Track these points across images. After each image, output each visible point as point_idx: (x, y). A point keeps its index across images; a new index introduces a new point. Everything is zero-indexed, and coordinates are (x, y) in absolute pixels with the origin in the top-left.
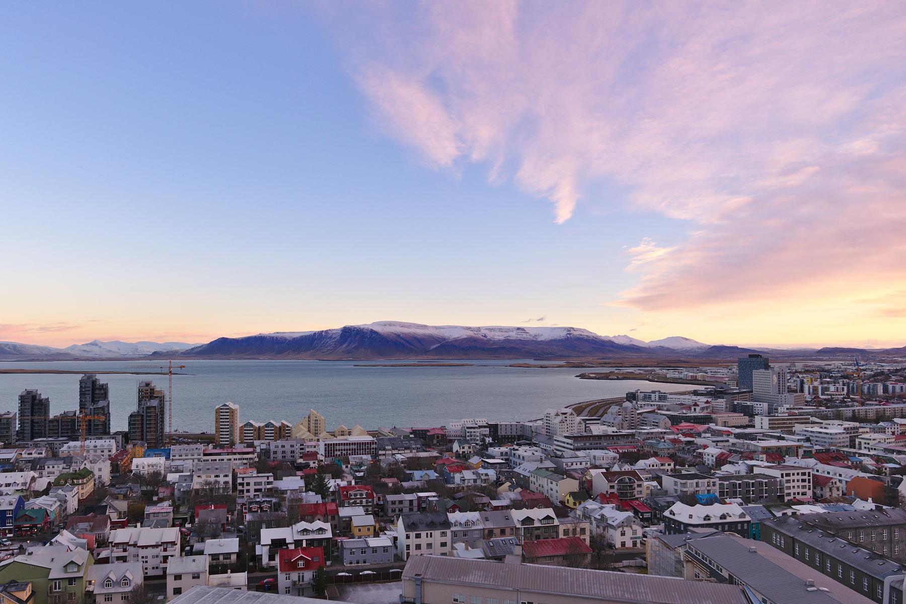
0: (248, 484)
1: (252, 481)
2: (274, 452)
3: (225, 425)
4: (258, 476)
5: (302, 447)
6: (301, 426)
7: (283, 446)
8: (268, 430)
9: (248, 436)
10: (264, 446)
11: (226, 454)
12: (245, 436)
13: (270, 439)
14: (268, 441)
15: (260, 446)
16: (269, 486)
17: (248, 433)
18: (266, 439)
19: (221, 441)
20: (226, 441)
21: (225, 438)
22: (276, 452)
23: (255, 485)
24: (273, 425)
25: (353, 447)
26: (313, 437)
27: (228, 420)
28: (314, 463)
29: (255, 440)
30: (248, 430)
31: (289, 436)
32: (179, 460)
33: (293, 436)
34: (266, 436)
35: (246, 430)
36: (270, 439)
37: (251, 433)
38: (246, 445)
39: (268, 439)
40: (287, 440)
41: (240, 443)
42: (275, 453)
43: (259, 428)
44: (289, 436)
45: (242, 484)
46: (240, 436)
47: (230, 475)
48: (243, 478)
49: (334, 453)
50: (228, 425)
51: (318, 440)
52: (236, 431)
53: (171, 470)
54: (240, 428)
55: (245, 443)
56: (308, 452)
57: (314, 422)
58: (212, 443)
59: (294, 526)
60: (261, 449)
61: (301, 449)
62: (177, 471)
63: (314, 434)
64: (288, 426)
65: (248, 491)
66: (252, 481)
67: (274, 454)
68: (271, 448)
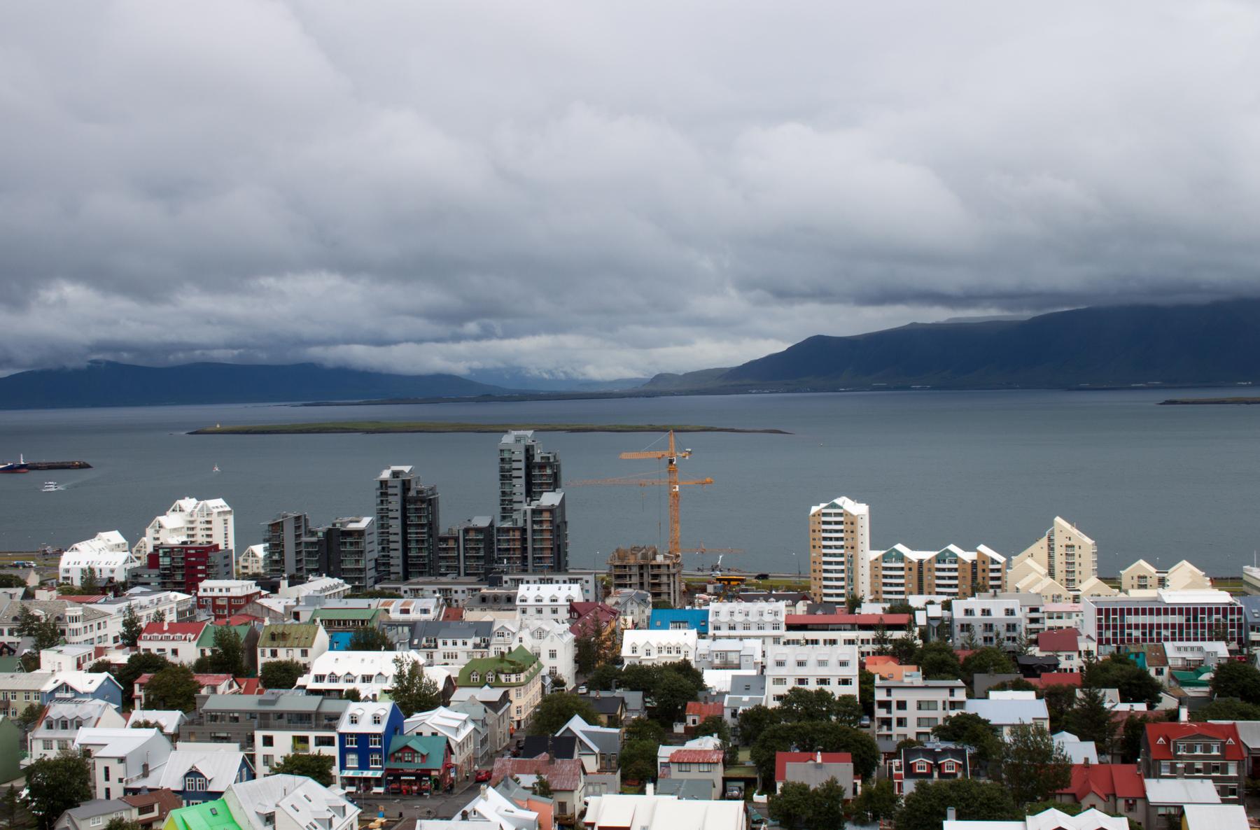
0: (902, 705)
1: (911, 698)
2: (962, 626)
3: (834, 555)
4: (926, 687)
5: (1034, 615)
6: (1029, 561)
7: (986, 612)
8: (944, 570)
9: (891, 585)
10: (936, 611)
11: (849, 627)
12: (885, 584)
13: (949, 594)
14: (945, 598)
15: (925, 609)
16: (953, 713)
17: (891, 577)
18: (938, 593)
19: (826, 595)
20: (838, 595)
21: (837, 587)
22: (968, 625)
23: (919, 708)
24: (955, 555)
25: (1171, 619)
26: (1061, 590)
27: (841, 543)
28: (1068, 658)
29: (911, 593)
30: (891, 569)
31: (999, 587)
32: (729, 637)
33: (1009, 586)
34: (938, 586)
35: (885, 569)
36: (949, 594)
37: (902, 577)
38: (887, 606)
39: (942, 593)
40: (995, 595)
41: (872, 601)
42: (966, 627)
43: (921, 562)
44: (999, 587)
45: (886, 705)
46: (872, 584)
47: (856, 681)
48: (889, 690)
49: (1115, 634)
50: (842, 555)
51: (1076, 599)
52: (861, 571)
53: (711, 662)
54: (871, 562)
55: (885, 601)
56: (1051, 629)
57: (1063, 551)
58: (805, 598)
59: (1029, 818)
60: (929, 619)
61: (1033, 621)
62: (726, 666)
63: (1064, 582)
64: (994, 561)
65: (901, 722)
66: (911, 698)
67: (962, 630)
68: (955, 616)
